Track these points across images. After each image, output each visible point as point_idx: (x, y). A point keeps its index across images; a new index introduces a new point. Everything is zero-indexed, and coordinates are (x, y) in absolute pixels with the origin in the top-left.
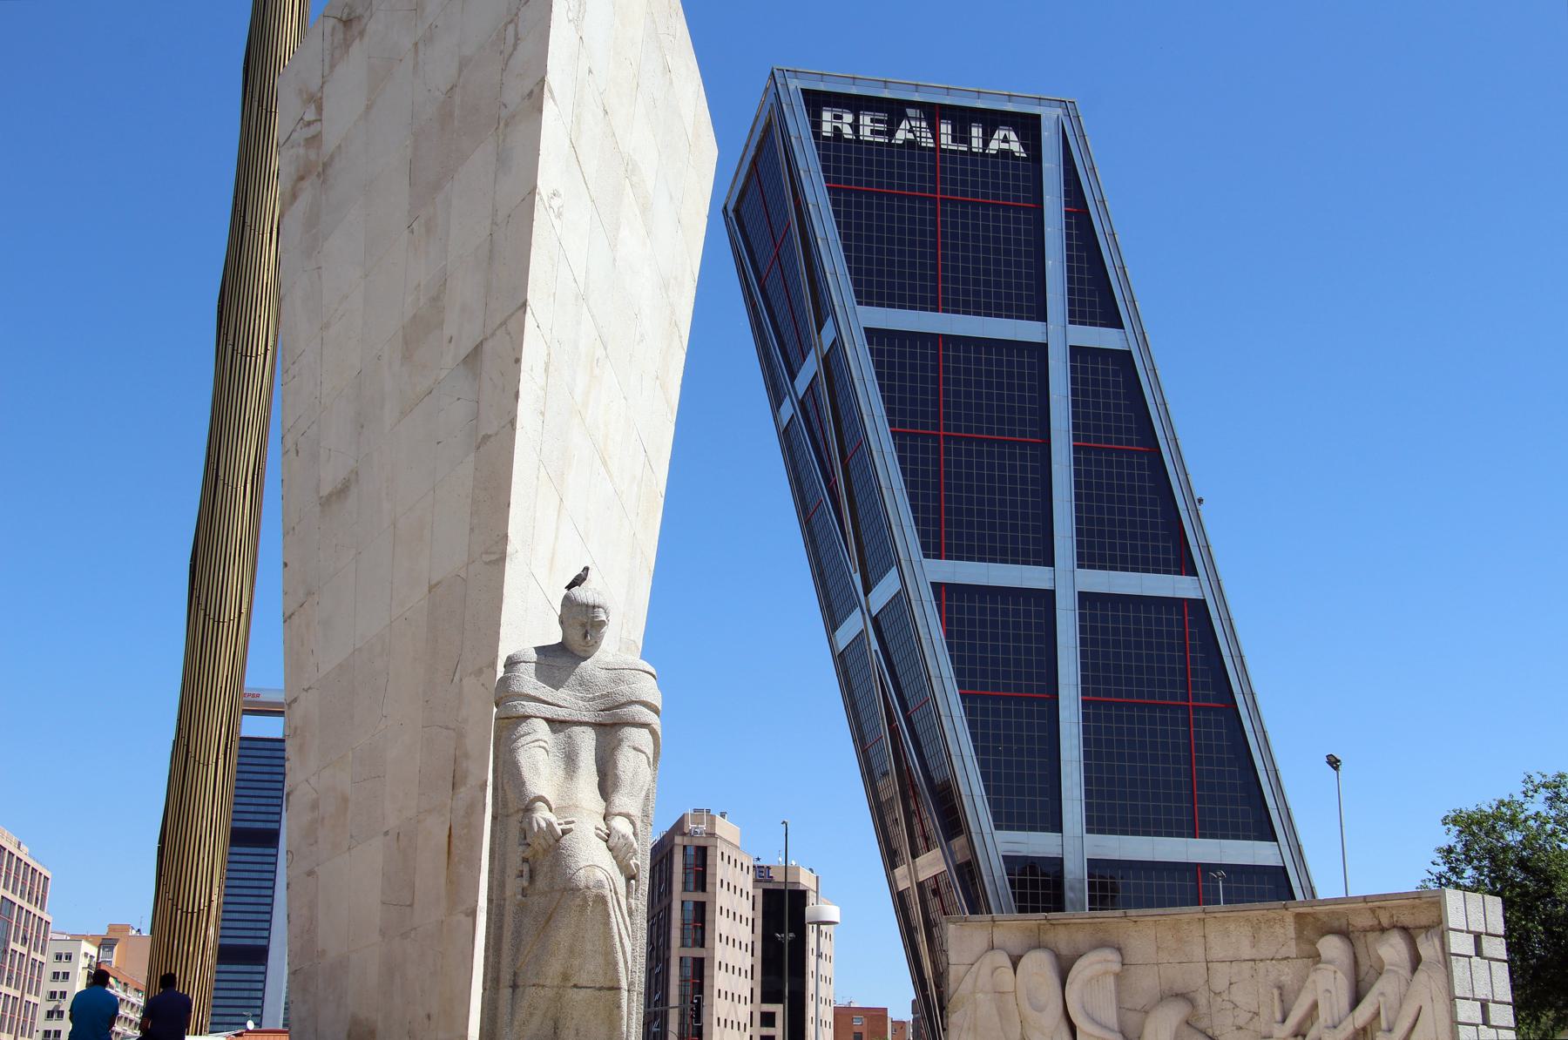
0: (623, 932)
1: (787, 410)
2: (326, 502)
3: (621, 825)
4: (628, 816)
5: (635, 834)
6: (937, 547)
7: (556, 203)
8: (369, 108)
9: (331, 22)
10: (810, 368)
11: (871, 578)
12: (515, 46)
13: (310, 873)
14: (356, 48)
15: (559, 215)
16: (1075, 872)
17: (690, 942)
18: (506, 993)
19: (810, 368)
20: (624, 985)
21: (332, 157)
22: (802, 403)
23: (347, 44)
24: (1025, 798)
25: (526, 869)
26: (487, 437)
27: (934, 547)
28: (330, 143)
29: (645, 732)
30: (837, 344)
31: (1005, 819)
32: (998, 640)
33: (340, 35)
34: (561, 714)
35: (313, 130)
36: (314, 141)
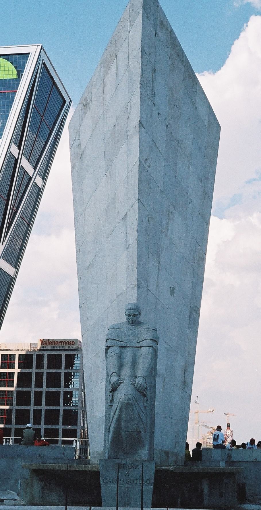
0: (141, 414)
7: (148, 162)
8: (92, 134)
9: (81, 105)
12: (131, 110)
13: (91, 391)
14: (88, 114)
15: (149, 167)
18: (108, 433)
20: (142, 430)
21: (83, 151)
23: (85, 113)
26: (129, 245)
28: (83, 147)
33: (83, 110)
34: (124, 344)
35: (77, 143)
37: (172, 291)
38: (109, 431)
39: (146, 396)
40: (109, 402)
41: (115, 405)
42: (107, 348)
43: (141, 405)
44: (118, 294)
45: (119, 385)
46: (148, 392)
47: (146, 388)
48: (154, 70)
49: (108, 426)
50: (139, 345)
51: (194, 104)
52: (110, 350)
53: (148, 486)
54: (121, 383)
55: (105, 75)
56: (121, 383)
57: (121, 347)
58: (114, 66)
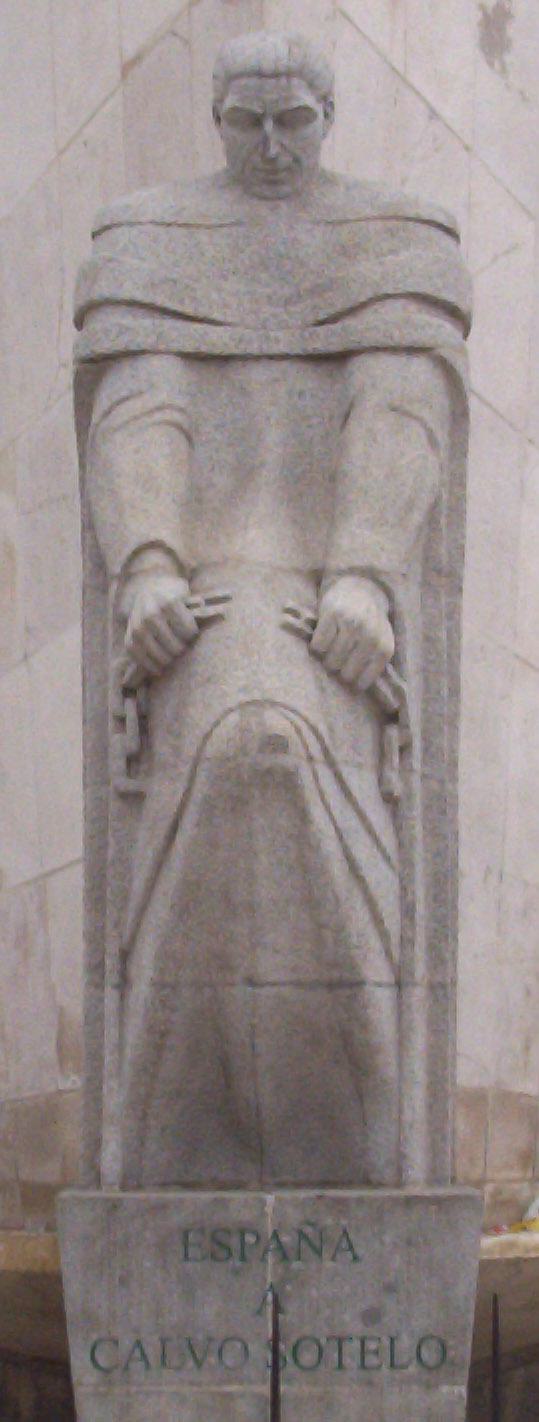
0: (363, 851)
3: (351, 600)
4: (370, 574)
5: (392, 617)
18: (111, 997)
20: (376, 970)
25: (130, 710)
29: (420, 367)
34: (217, 340)
38: (124, 983)
39: (389, 717)
40: (117, 764)
41: (163, 793)
42: (93, 370)
43: (363, 785)
44: (130, 51)
45: (190, 642)
46: (412, 687)
47: (396, 661)
49: (112, 948)
50: (326, 340)
52: (115, 385)
53: (429, 1386)
54: (203, 623)
56: (203, 623)
57: (196, 359)
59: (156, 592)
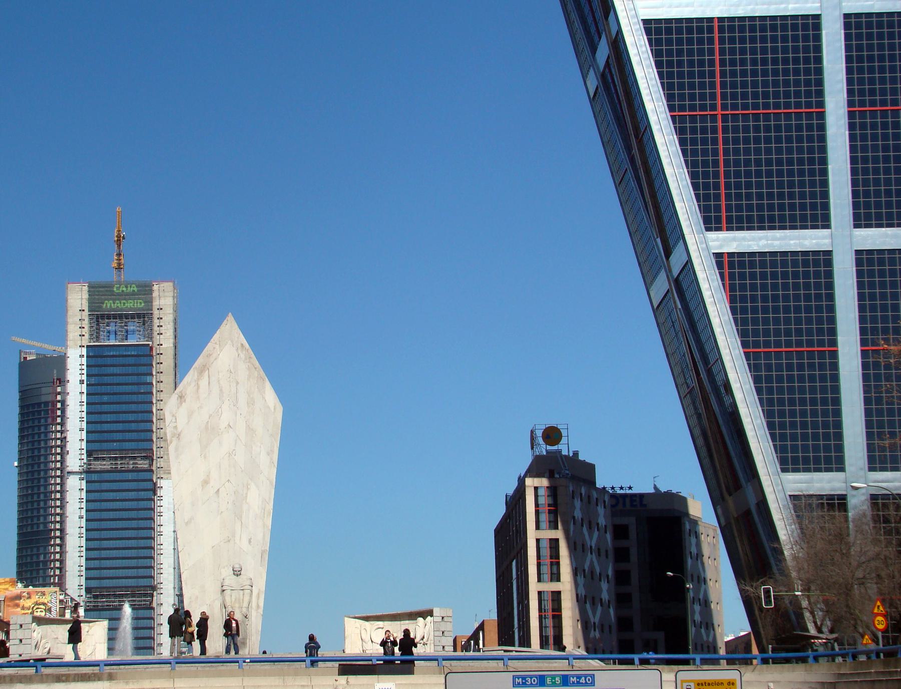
1: (593, 82)
2: (187, 524)
6: (718, 220)
10: (603, 51)
11: (671, 243)
16: (857, 503)
17: (546, 577)
19: (603, 51)
22: (603, 76)
23: (181, 403)
24: (809, 440)
27: (711, 222)
28: (179, 430)
30: (619, 32)
31: (789, 461)
32: (782, 299)
35: (174, 425)
36: (176, 427)
37: (250, 542)
48: (237, 383)
51: (264, 398)
55: (198, 379)
58: (206, 377)
59: (230, 610)
